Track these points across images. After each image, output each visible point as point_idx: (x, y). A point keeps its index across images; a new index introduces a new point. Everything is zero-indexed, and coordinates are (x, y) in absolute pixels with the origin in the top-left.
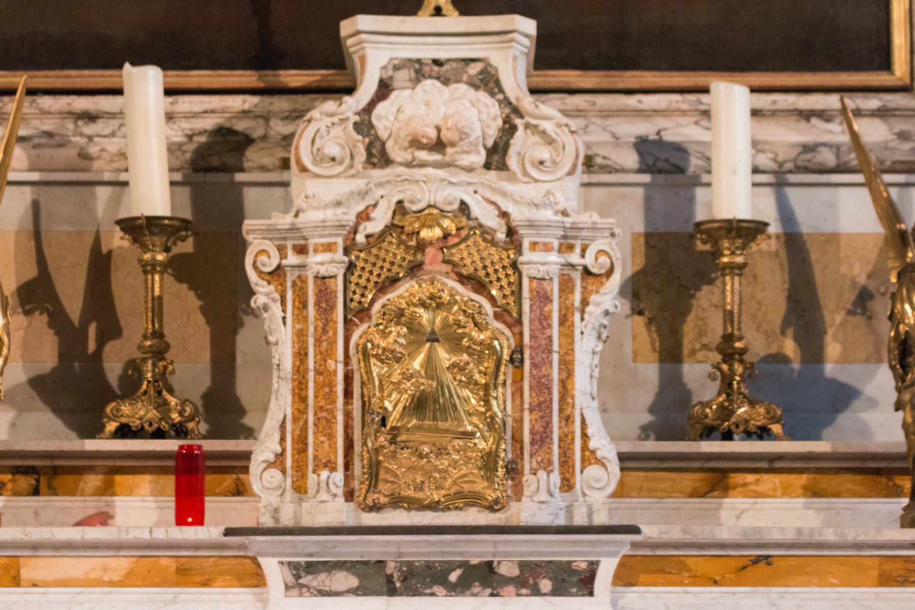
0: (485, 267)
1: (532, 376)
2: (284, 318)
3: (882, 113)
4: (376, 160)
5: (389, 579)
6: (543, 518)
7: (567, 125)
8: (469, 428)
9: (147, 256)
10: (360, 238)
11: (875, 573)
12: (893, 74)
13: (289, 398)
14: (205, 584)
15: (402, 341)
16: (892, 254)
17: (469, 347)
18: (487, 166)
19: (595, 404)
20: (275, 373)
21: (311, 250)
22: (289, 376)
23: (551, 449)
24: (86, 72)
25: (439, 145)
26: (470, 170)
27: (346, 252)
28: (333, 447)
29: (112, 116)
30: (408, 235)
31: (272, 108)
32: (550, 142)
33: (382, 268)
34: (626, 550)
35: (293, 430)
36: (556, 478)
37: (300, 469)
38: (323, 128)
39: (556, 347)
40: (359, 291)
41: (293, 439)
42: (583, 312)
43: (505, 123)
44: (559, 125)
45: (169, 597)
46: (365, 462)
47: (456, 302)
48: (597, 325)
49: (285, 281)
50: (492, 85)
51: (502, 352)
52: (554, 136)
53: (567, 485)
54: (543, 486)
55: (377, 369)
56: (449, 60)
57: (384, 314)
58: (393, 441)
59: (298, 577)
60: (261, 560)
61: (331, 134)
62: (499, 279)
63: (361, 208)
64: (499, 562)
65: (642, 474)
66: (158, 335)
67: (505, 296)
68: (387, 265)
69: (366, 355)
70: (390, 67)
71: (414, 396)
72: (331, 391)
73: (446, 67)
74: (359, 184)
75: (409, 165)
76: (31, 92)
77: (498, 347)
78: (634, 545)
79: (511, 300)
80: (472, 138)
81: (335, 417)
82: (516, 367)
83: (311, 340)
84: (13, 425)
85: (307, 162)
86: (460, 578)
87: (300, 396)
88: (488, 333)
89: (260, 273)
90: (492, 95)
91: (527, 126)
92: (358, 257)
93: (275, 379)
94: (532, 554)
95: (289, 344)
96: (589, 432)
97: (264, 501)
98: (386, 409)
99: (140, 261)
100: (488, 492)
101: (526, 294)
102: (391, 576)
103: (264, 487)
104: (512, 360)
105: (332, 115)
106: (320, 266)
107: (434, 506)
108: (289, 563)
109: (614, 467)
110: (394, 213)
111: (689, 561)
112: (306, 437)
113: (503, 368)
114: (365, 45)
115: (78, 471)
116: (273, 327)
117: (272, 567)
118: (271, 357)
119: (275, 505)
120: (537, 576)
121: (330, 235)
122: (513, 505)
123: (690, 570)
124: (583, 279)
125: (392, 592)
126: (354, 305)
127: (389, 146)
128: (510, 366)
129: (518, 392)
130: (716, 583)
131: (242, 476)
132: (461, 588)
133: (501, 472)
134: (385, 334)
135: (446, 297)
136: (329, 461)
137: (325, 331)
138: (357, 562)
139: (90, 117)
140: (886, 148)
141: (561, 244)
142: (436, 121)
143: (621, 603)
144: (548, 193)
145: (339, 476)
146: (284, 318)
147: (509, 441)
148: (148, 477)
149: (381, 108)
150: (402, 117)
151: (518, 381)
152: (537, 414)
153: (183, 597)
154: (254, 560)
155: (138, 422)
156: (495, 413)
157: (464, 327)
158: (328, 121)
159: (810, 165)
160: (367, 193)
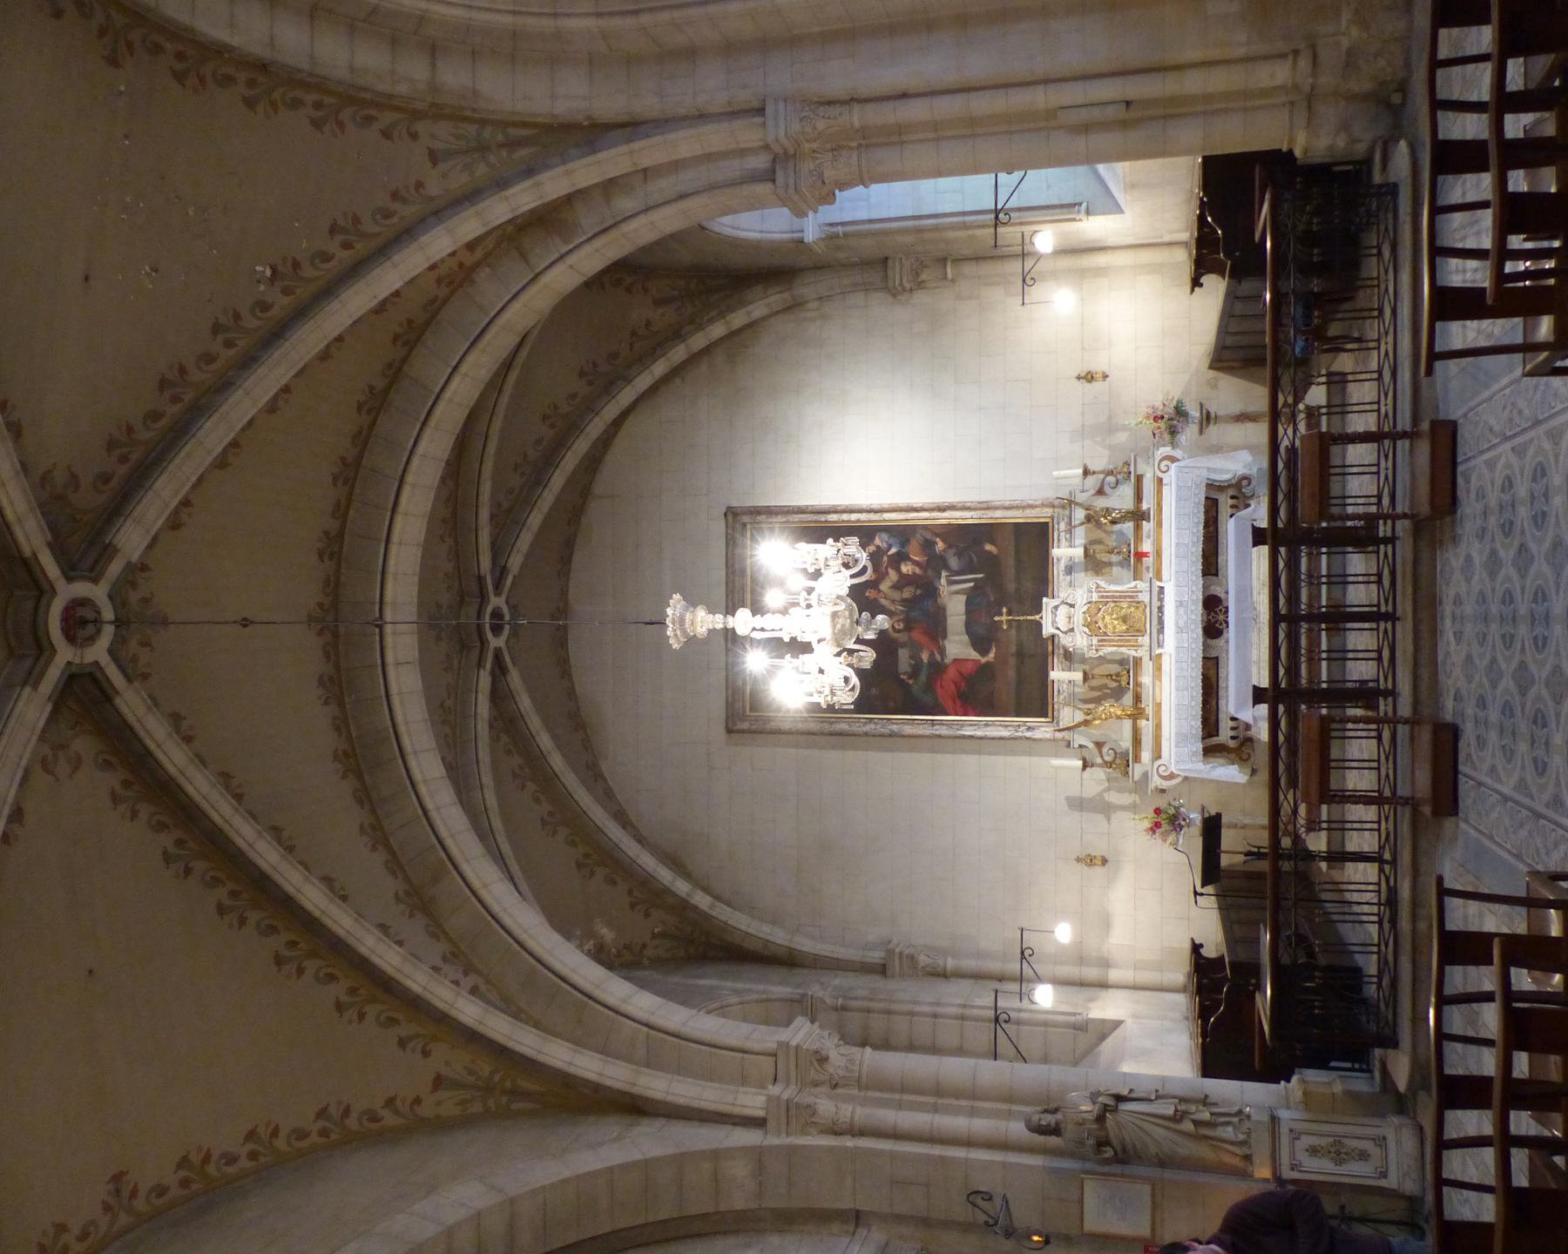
3: (1058, 524)
25: (1070, 618)
74: (1078, 634)
117: (1158, 651)
125: (1163, 627)
132: (1162, 613)
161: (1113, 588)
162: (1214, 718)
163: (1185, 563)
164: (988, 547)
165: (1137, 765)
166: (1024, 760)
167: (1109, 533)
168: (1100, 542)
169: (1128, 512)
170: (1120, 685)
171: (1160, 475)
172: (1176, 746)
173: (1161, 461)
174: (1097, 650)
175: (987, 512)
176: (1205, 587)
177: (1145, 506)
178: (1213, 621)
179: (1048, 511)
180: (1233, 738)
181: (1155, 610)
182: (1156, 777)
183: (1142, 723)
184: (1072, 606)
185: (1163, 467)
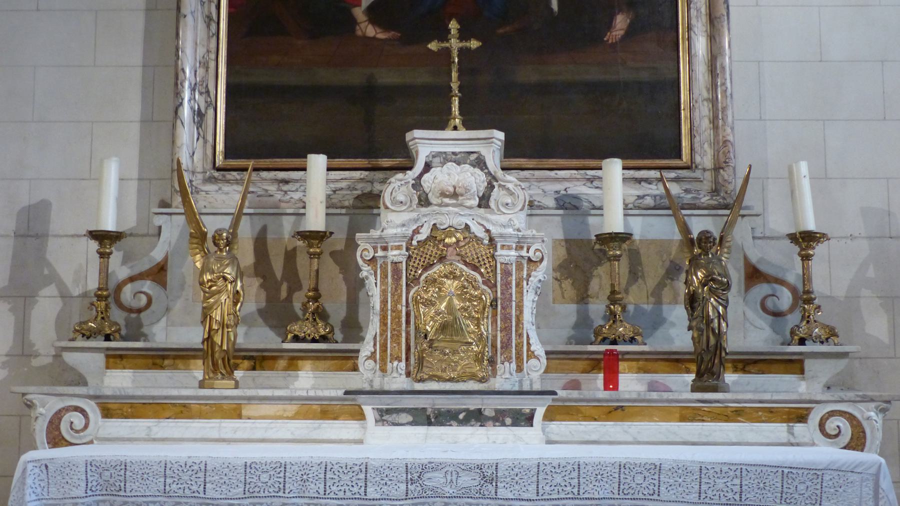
0: (478, 258)
1: (501, 313)
2: (376, 283)
3: (676, 180)
4: (423, 203)
5: (428, 417)
6: (507, 387)
7: (520, 185)
8: (470, 340)
10: (414, 243)
11: (678, 415)
12: (683, 161)
13: (378, 324)
14: (335, 419)
16: (686, 250)
17: (470, 299)
18: (479, 206)
19: (534, 327)
20: (372, 311)
21: (390, 249)
22: (378, 313)
23: (511, 351)
24: (284, 160)
25: (455, 195)
26: (470, 208)
27: (408, 249)
28: (400, 349)
29: (297, 181)
30: (439, 241)
31: (374, 177)
32: (511, 193)
33: (425, 258)
34: (550, 403)
35: (380, 341)
36: (514, 366)
37: (383, 360)
38: (397, 187)
39: (514, 299)
41: (380, 345)
42: (528, 280)
43: (488, 184)
44: (516, 186)
45: (316, 425)
46: (416, 357)
47: (463, 275)
49: (377, 264)
50: (482, 165)
51: (486, 301)
52: (513, 191)
53: (520, 369)
56: (461, 152)
57: (426, 282)
58: (430, 347)
59: (382, 416)
60: (363, 407)
61: (401, 190)
62: (485, 264)
63: (415, 227)
64: (485, 409)
65: (558, 361)
66: (316, 289)
68: (428, 256)
69: (417, 302)
70: (431, 156)
71: (441, 324)
72: (399, 321)
73: (459, 156)
74: (414, 215)
75: (440, 205)
76: (256, 169)
77: (484, 299)
78: (553, 400)
79: (491, 274)
80: (472, 192)
82: (494, 309)
83: (389, 295)
84: (246, 334)
85: (389, 205)
86: (465, 417)
87: (383, 323)
89: (364, 260)
90: (482, 170)
91: (500, 186)
92: (413, 252)
93: (371, 314)
94: (501, 405)
96: (531, 342)
97: (365, 376)
98: (427, 330)
99: (308, 252)
100: (479, 373)
101: (499, 271)
102: (430, 416)
103: (365, 369)
104: (491, 305)
105: (401, 180)
106: (394, 257)
107: (451, 380)
108: (377, 409)
109: (544, 361)
110: (432, 230)
111: (583, 409)
112: (387, 344)
113: (487, 310)
114: (418, 145)
115: (275, 358)
116: (371, 287)
117: (368, 410)
118: (369, 302)
119: (371, 378)
121: (399, 241)
122: (492, 379)
123: (582, 413)
124: (528, 264)
125: (430, 424)
126: (411, 276)
127: (430, 195)
128: (490, 308)
129: (494, 322)
130: (595, 420)
131: (356, 361)
132: (465, 422)
133: (486, 362)
134: (426, 292)
135: (458, 273)
136: (398, 357)
137: (396, 290)
138: (413, 408)
139: (286, 182)
140: (679, 197)
142: (453, 183)
143: (547, 430)
144: (510, 220)
145: (403, 364)
146: (376, 283)
147: (490, 347)
148: (310, 362)
149: (426, 176)
150: (436, 181)
151: (495, 315)
152: (504, 333)
153: (324, 425)
154: (359, 406)
156: (482, 332)
157: (467, 288)
158: (399, 183)
159: (641, 206)
160: (418, 220)
164: (621, 22)
165: (100, 358)
166: (133, 109)
167: (657, 295)
168: (635, 274)
169: (719, 335)
170: (296, 319)
171: (815, 418)
172: (89, 464)
173: (851, 418)
174: (373, 260)
175: (704, 19)
179: (706, 159)
181: (473, 403)
182: (56, 404)
184: (484, 201)
185: (832, 425)
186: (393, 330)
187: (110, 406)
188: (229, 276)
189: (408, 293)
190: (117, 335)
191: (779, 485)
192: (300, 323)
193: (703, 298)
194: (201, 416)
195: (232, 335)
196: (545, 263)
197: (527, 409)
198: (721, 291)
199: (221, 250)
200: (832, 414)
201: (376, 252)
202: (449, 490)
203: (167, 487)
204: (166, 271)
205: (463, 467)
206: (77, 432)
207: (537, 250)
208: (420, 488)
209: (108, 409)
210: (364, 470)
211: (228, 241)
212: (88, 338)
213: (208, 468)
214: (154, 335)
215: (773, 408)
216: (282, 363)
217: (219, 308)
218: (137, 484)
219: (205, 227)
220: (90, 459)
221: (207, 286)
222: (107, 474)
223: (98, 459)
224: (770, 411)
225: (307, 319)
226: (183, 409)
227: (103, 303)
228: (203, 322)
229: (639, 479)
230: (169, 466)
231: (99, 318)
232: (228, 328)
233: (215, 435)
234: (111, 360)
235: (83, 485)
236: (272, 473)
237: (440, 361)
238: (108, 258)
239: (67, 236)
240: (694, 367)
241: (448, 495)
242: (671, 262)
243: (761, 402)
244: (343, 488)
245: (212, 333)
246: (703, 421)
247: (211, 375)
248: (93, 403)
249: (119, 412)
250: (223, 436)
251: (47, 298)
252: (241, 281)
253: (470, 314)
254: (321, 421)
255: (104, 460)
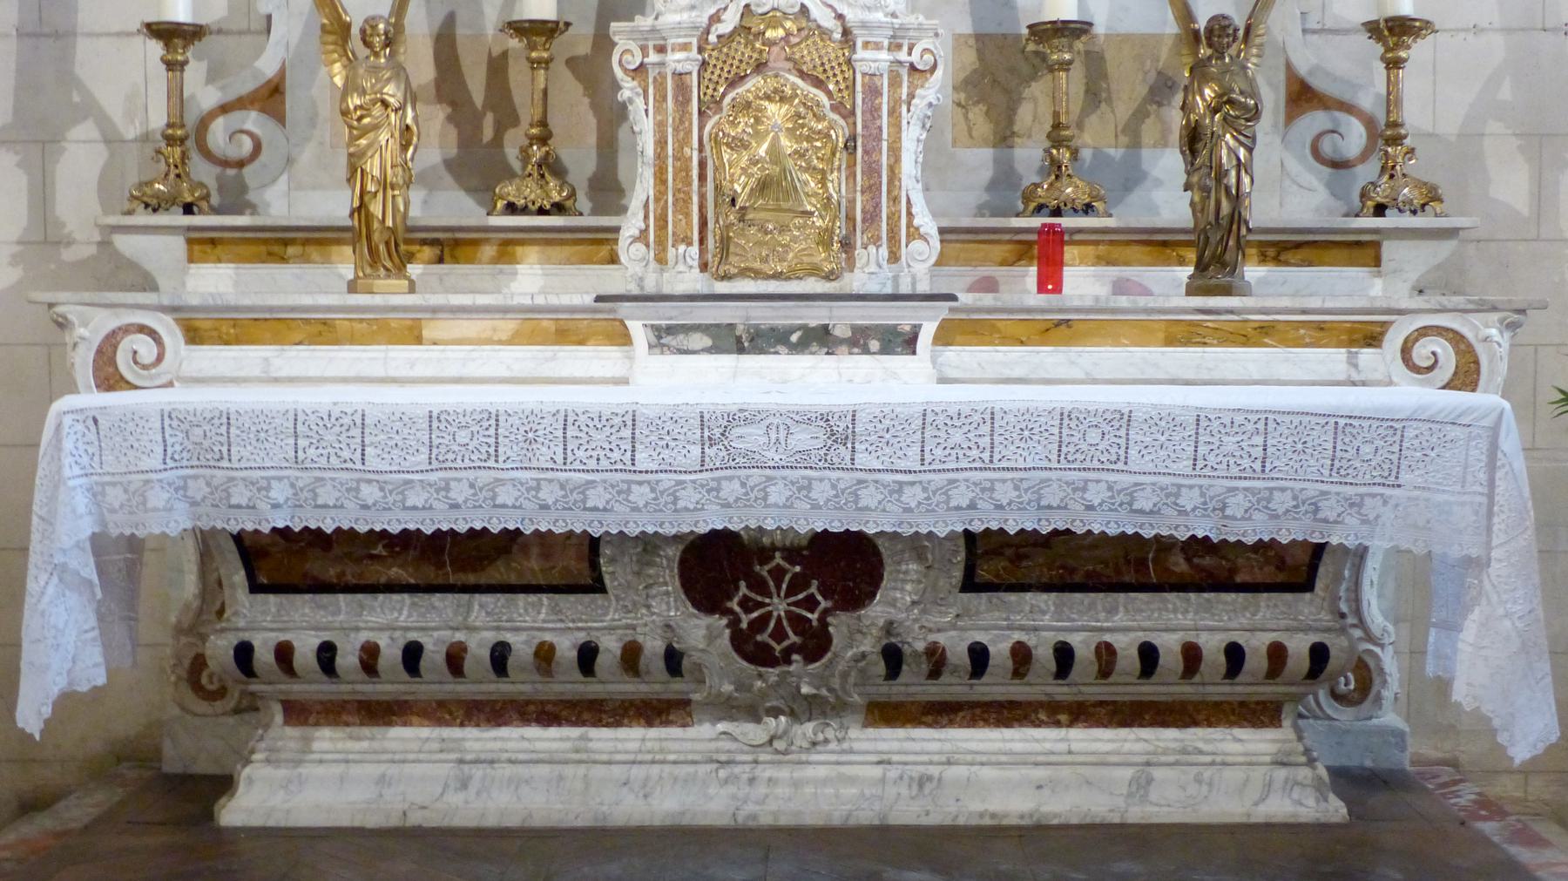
0: (823, 64)
1: (864, 161)
2: (646, 111)
5: (739, 340)
6: (873, 288)
8: (809, 208)
9: (534, 55)
10: (712, 38)
11: (1161, 335)
13: (652, 181)
14: (581, 343)
15: (749, 130)
16: (1185, 51)
19: (920, 186)
20: (640, 160)
27: (700, 50)
28: (689, 224)
33: (732, 65)
34: (945, 314)
36: (884, 252)
37: (661, 243)
39: (885, 136)
40: (711, 86)
42: (909, 104)
45: (549, 354)
47: (797, 95)
48: (921, 116)
53: (894, 257)
54: (873, 259)
55: (726, 155)
58: (741, 220)
59: (659, 337)
60: (628, 323)
62: (835, 75)
63: (712, 11)
64: (834, 326)
65: (958, 245)
66: (543, 123)
67: (840, 91)
68: (736, 63)
78: (951, 310)
79: (845, 94)
81: (691, 198)
83: (670, 130)
84: (425, 202)
86: (800, 338)
88: (826, 123)
89: (626, 71)
93: (639, 164)
94: (863, 317)
95: (651, 133)
96: (914, 211)
97: (630, 271)
99: (528, 59)
100: (825, 264)
101: (859, 88)
102: (741, 337)
107: (777, 276)
108: (652, 326)
110: (742, 15)
111: (999, 324)
112: (666, 216)
113: (838, 155)
115: (475, 243)
116: (637, 118)
117: (637, 329)
118: (635, 145)
120: (867, 337)
121: (686, 36)
122: (847, 275)
123: (999, 331)
125: (741, 350)
126: (708, 97)
128: (845, 153)
130: (1022, 343)
132: (800, 347)
134: (733, 124)
135: (788, 91)
137: (682, 122)
138: (711, 325)
141: (890, 44)
145: (694, 250)
146: (646, 111)
151: (852, 165)
152: (867, 195)
153: (562, 354)
154: (622, 322)
155: (523, 201)
161: (912, 137)
162: (331, 573)
163: (1035, 454)
165: (178, 244)
167: (1132, 133)
168: (1095, 95)
169: (1237, 198)
170: (510, 175)
171: (1394, 340)
172: (167, 416)
173: (1456, 338)
176: (918, 545)
177: (1253, 272)
178: (763, 571)
180: (244, 653)
181: (814, 316)
182: (106, 322)
183: (345, 265)
186: (677, 191)
187: (197, 324)
188: (391, 100)
189: (701, 129)
190: (204, 205)
191: (1329, 446)
192: (517, 181)
193: (1213, 133)
194: (353, 339)
195: (400, 201)
196: (939, 73)
197: (906, 325)
198: (1243, 122)
199: (376, 55)
200: (1424, 332)
201: (645, 54)
202: (773, 456)
203: (300, 453)
204: (283, 94)
205: (797, 418)
206: (145, 367)
207: (926, 50)
208: (724, 453)
209: (196, 330)
210: (629, 423)
211: (387, 38)
212: (155, 210)
213: (367, 421)
214: (268, 205)
215: (1324, 322)
216: (489, 251)
217: (377, 156)
218: (249, 448)
219: (346, 13)
220: (167, 409)
221: (355, 117)
222: (198, 431)
223: (181, 407)
224: (1320, 327)
225: (530, 175)
226: (321, 328)
227: (178, 150)
228: (350, 180)
229: (1094, 436)
230: (301, 418)
231: (172, 176)
232: (393, 189)
233: (379, 371)
234: (197, 248)
235: (160, 450)
236: (475, 428)
237: (759, 243)
238: (182, 71)
239: (109, 34)
240: (1192, 255)
241: (771, 464)
242: (1159, 73)
243: (1304, 312)
244: (594, 454)
245: (366, 198)
246: (1205, 344)
247: (368, 270)
248: (168, 319)
249: (215, 334)
250: (393, 373)
251: (82, 145)
252: (414, 108)
253: (809, 162)
254: (556, 348)
255: (191, 409)
